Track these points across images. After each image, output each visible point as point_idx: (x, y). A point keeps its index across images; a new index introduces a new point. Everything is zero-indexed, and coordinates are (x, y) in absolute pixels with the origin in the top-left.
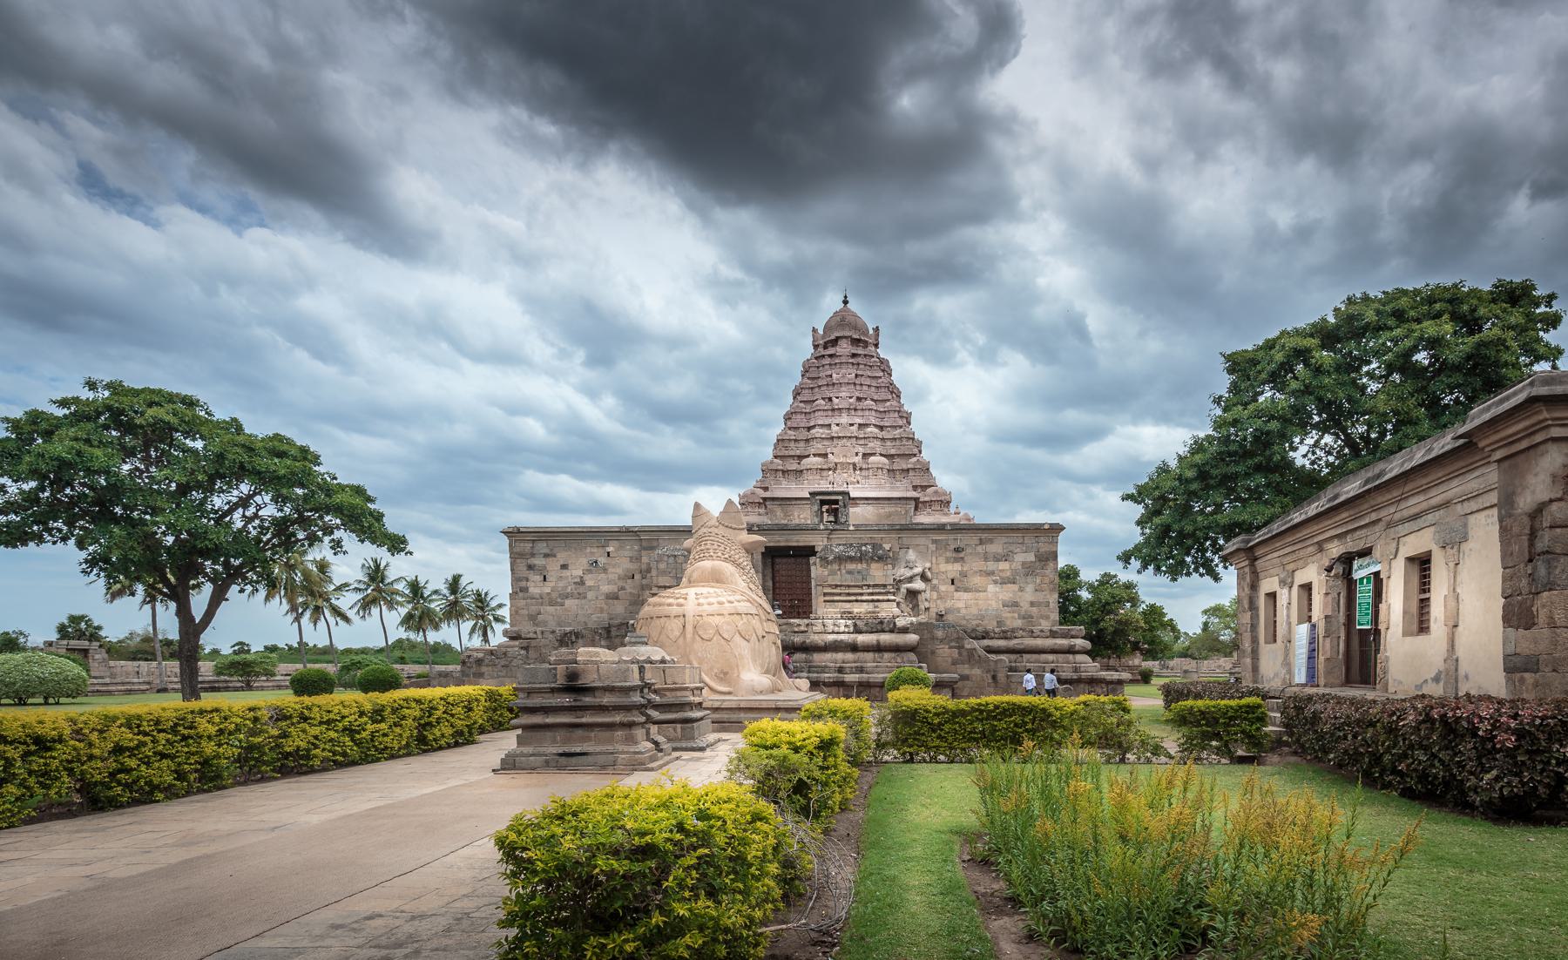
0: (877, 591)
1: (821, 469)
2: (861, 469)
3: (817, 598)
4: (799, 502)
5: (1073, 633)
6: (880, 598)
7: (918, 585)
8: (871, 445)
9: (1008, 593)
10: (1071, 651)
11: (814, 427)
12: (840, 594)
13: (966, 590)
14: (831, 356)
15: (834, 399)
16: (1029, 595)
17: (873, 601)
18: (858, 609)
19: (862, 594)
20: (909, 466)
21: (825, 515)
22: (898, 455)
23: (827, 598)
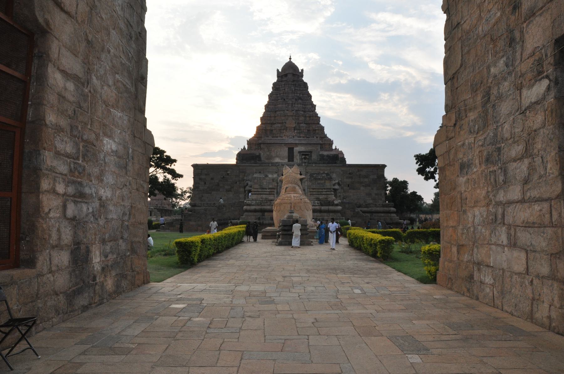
1: (281, 129)
2: (297, 129)
4: (274, 145)
6: (329, 193)
7: (337, 187)
11: (277, 111)
12: (315, 192)
13: (354, 189)
17: (326, 194)
18: (321, 197)
19: (322, 192)
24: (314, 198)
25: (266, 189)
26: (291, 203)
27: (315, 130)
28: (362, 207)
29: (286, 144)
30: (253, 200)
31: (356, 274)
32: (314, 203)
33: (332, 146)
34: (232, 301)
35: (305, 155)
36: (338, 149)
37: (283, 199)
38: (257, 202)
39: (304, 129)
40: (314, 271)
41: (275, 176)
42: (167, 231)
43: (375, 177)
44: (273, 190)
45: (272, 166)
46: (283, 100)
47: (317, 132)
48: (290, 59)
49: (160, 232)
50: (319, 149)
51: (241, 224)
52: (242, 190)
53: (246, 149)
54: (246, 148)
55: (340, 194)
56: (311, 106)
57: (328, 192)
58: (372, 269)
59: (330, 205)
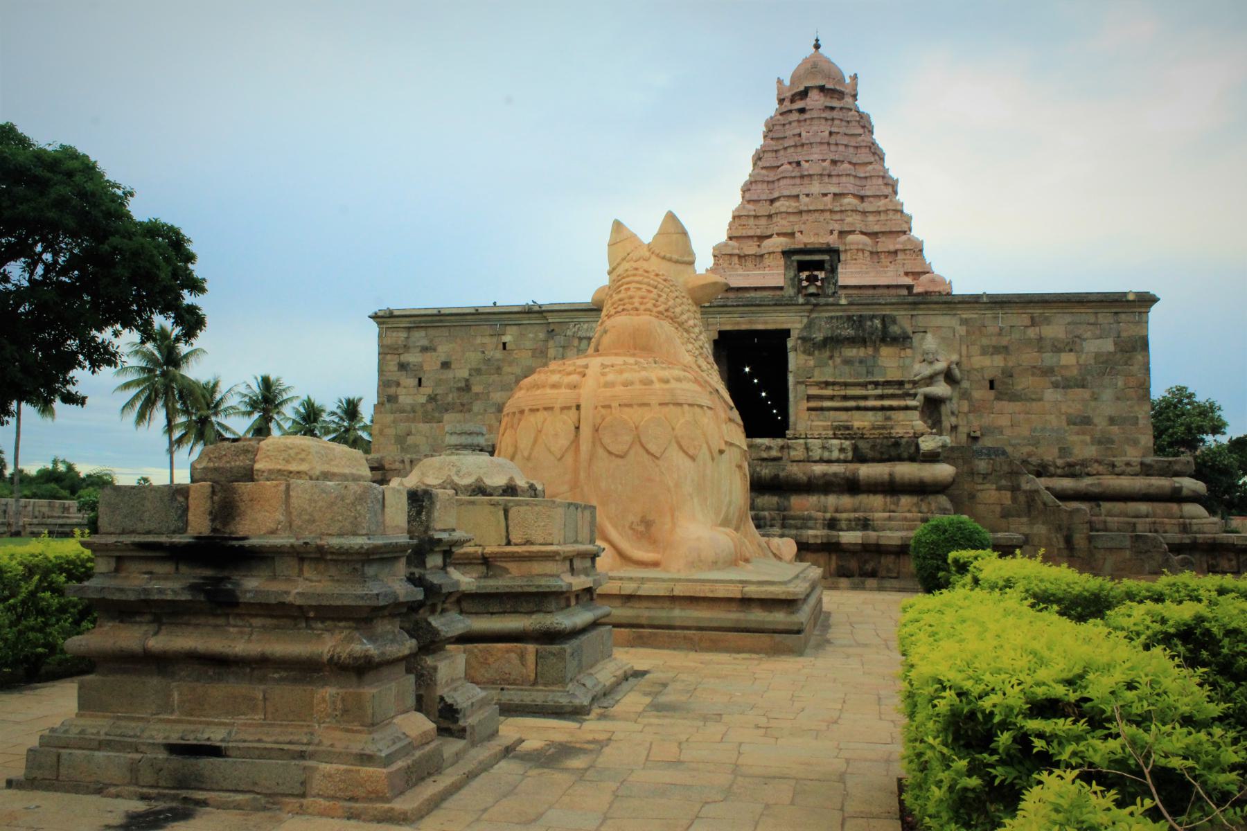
0: (890, 391)
3: (796, 403)
5: (1177, 467)
6: (894, 403)
7: (941, 389)
8: (849, 220)
9: (1074, 402)
10: (1176, 497)
12: (832, 398)
13: (1014, 397)
14: (802, 111)
16: (1107, 406)
17: (883, 408)
18: (861, 421)
19: (865, 398)
20: (898, 247)
21: (805, 284)
22: (883, 233)
23: (813, 404)
24: (825, 428)
28: (1052, 476)
32: (824, 448)
39: (858, 250)
43: (1108, 346)
55: (953, 420)
57: (893, 396)
59: (900, 459)
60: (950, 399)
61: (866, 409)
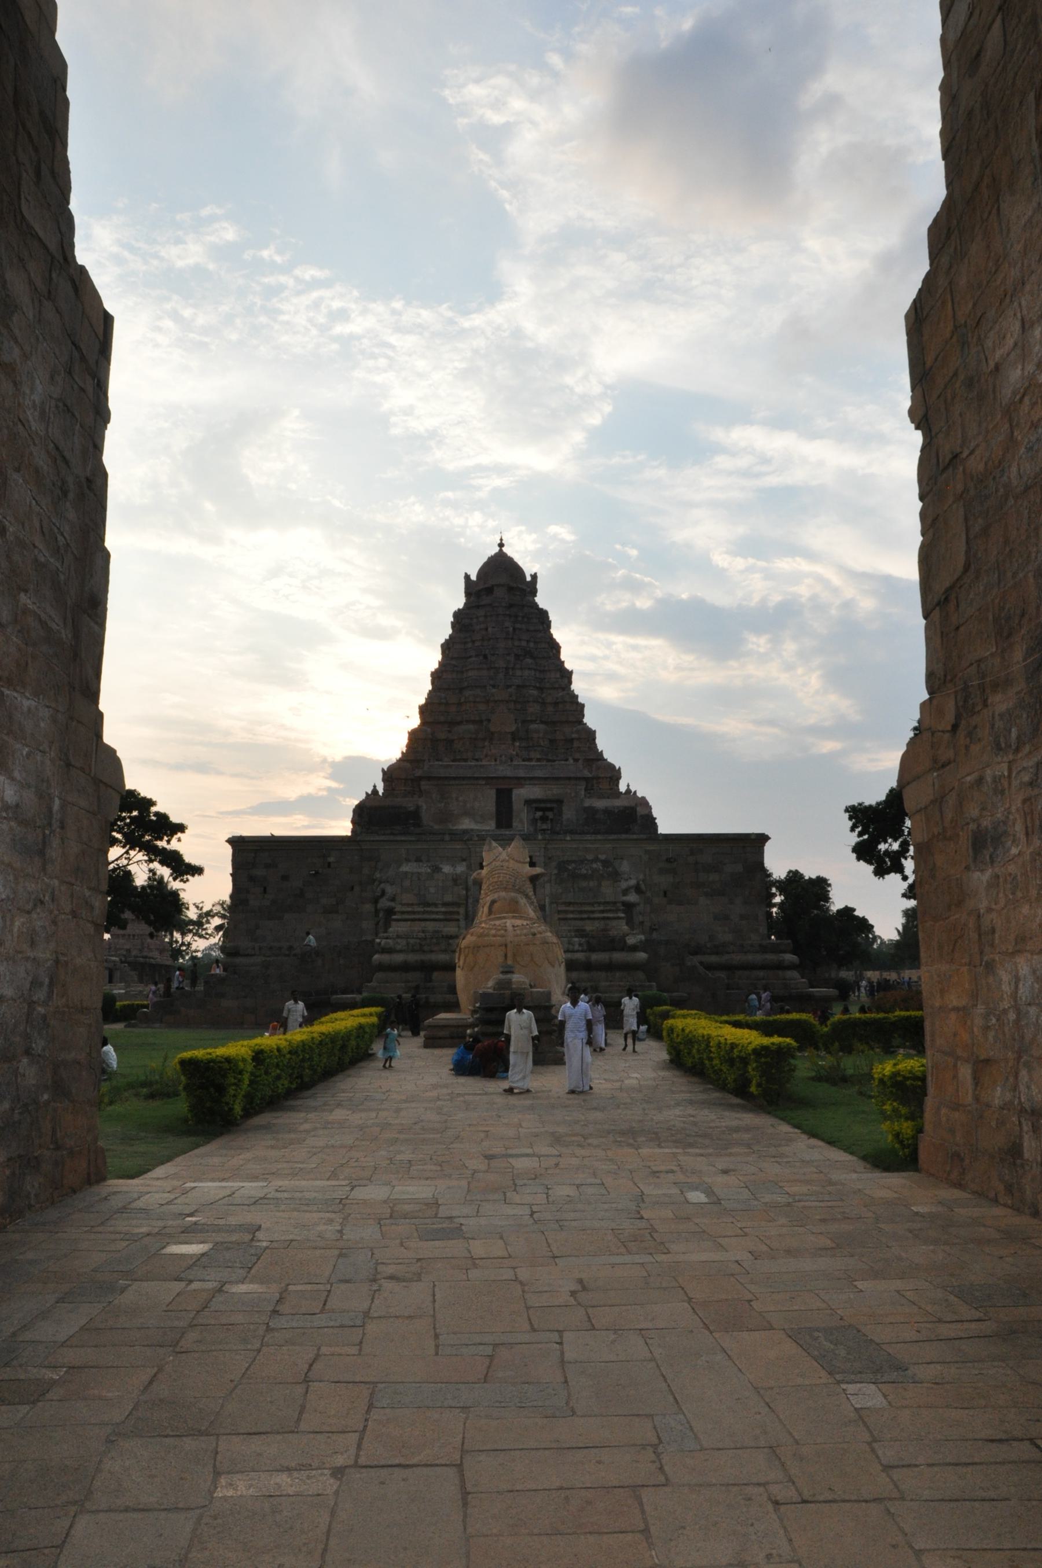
0: (608, 908)
7: (632, 898)
12: (572, 912)
15: (489, 656)
17: (604, 918)
18: (589, 927)
19: (593, 912)
24: (570, 931)
25: (436, 905)
26: (506, 946)
27: (571, 741)
29: (488, 779)
30: (398, 937)
31: (691, 1145)
32: (569, 943)
33: (617, 785)
34: (340, 1232)
35: (543, 810)
36: (635, 792)
37: (481, 935)
38: (412, 941)
39: (539, 738)
40: (573, 1138)
41: (461, 868)
42: (158, 1025)
44: (455, 909)
45: (451, 840)
46: (481, 658)
47: (576, 744)
48: (501, 545)
49: (136, 1030)
50: (583, 792)
51: (365, 1004)
52: (368, 907)
53: (381, 794)
54: (381, 790)
55: (641, 918)
56: (558, 676)
58: (737, 1130)
59: (614, 949)
60: (638, 904)
61: (594, 919)
